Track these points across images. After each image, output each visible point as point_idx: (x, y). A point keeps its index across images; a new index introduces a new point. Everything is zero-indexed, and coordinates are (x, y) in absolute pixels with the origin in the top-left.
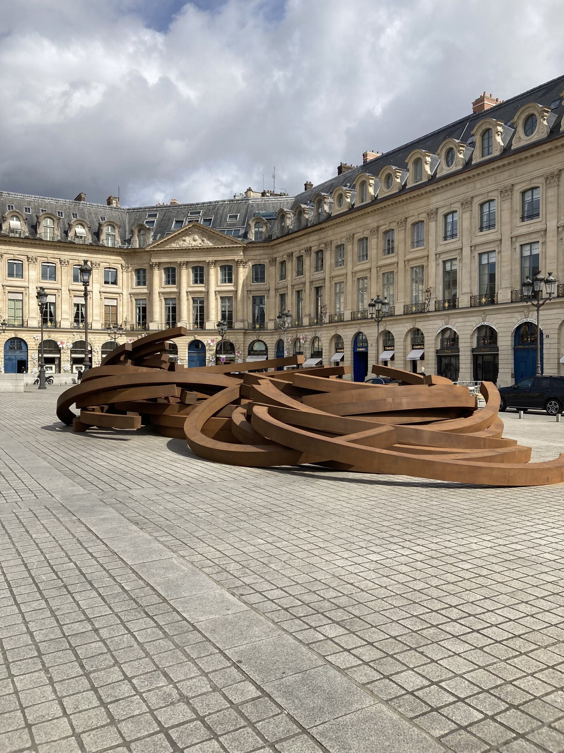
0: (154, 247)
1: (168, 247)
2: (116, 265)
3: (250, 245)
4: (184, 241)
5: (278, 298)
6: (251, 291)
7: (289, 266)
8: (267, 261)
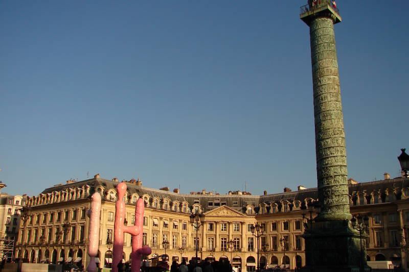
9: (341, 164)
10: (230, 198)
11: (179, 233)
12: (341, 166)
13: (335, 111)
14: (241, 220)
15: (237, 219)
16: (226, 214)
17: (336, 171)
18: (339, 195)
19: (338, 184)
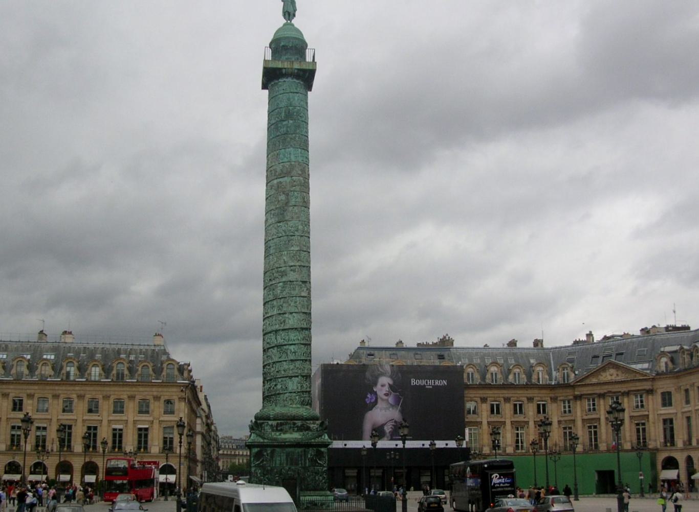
0: (578, 382)
1: (588, 381)
2: (547, 398)
3: (658, 377)
4: (602, 376)
5: (685, 421)
6: (661, 414)
7: (691, 393)
8: (673, 389)
9: (277, 327)
10: (633, 343)
11: (527, 423)
12: (276, 331)
13: (275, 240)
14: (647, 386)
15: (638, 384)
16: (614, 378)
17: (269, 341)
18: (271, 380)
19: (270, 361)
